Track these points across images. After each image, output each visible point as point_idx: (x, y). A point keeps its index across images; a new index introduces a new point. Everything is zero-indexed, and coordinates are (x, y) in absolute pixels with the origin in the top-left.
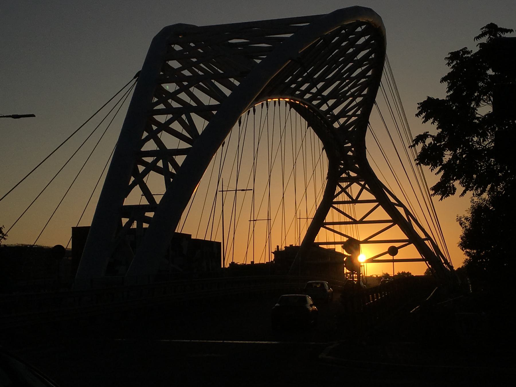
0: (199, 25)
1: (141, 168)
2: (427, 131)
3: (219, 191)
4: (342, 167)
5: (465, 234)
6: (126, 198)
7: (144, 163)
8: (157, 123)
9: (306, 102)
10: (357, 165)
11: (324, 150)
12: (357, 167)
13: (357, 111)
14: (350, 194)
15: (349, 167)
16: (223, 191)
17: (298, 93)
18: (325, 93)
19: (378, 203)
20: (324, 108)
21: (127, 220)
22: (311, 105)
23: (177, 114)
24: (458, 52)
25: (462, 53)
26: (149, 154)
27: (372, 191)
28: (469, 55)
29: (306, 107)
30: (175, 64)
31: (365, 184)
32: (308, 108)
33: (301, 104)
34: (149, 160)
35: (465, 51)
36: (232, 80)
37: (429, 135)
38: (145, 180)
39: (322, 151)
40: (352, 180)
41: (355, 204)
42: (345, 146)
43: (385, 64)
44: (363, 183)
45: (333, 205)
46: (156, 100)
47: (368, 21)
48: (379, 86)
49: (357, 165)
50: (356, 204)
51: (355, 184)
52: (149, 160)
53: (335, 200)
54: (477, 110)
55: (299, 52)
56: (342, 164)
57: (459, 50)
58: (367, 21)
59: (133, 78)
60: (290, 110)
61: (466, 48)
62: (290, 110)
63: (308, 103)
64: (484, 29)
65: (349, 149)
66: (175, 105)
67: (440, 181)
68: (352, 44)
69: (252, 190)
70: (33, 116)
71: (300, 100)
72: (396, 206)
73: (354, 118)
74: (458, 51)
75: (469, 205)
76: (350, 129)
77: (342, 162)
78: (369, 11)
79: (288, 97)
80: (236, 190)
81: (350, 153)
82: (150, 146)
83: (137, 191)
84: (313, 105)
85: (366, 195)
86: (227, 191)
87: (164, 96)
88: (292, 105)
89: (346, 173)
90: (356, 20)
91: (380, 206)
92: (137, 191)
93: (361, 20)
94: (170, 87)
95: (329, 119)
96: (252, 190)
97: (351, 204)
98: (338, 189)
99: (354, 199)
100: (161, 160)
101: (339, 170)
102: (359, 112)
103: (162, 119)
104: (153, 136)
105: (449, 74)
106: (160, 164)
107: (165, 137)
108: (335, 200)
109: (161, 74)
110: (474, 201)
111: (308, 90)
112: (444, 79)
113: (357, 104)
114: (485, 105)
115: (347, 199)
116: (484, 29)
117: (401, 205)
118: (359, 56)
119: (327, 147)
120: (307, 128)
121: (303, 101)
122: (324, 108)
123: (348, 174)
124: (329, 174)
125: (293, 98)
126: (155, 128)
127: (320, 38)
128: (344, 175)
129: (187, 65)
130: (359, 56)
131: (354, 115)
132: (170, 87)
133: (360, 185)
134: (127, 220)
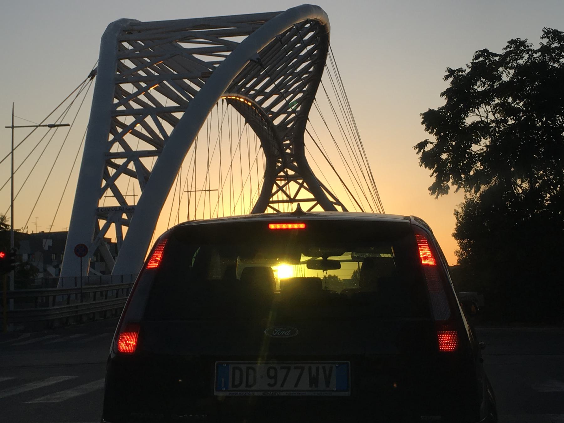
0: (143, 19)
1: (112, 171)
2: (427, 139)
3: (185, 192)
4: (280, 165)
5: (458, 226)
6: (100, 198)
7: (114, 166)
8: (122, 125)
9: (249, 99)
10: (295, 164)
11: (262, 148)
12: (295, 165)
13: (297, 107)
14: (289, 194)
15: (286, 165)
16: (188, 192)
17: (252, 92)
18: (268, 90)
19: (315, 202)
20: (265, 105)
21: (105, 221)
22: (254, 102)
23: (140, 116)
24: (455, 71)
25: (457, 71)
26: (118, 155)
27: (310, 190)
28: (463, 74)
29: (248, 104)
30: (128, 63)
31: (303, 183)
32: (252, 106)
33: (246, 102)
34: (120, 162)
35: (460, 70)
36: (186, 81)
37: (429, 142)
38: (116, 183)
39: (259, 147)
40: (289, 179)
41: (293, 203)
42: (284, 143)
43: (328, 61)
44: (300, 181)
45: (270, 204)
46: (116, 101)
47: (317, 19)
48: (320, 82)
49: (295, 164)
50: (294, 203)
51: (292, 183)
52: (120, 162)
53: (271, 200)
54: (465, 120)
55: (258, 52)
56: (279, 162)
57: (455, 69)
58: (315, 19)
59: (87, 77)
60: (227, 107)
61: (462, 68)
62: (227, 107)
63: (252, 101)
64: (478, 53)
65: (288, 146)
66: (136, 106)
67: (435, 182)
68: (300, 40)
69: (217, 190)
70: (68, 125)
71: (245, 97)
72: (335, 206)
73: (293, 115)
74: (454, 70)
75: (464, 201)
76: (289, 126)
77: (281, 160)
78: (317, 9)
79: (235, 95)
80: (209, 190)
81: (288, 151)
82: (117, 148)
83: (109, 192)
84: (256, 102)
85: (305, 194)
86: (202, 191)
87: (125, 97)
88: (229, 101)
89: (284, 172)
90: (307, 19)
91: (319, 205)
92: (109, 192)
93: (311, 19)
94: (129, 88)
95: (270, 116)
96: (217, 190)
97: (289, 203)
98: (275, 188)
99: (292, 197)
100: (132, 163)
101: (277, 168)
102: (298, 109)
103: (128, 120)
104: (119, 139)
105: (447, 89)
106: (132, 166)
107: (129, 138)
108: (271, 200)
109: (118, 74)
110: (467, 198)
111: (253, 87)
112: (443, 95)
113: (297, 101)
114: (473, 115)
115: (285, 198)
116: (478, 53)
117: (339, 203)
118: (302, 53)
119: (265, 145)
120: (245, 125)
121: (247, 98)
122: (265, 105)
123: (286, 173)
124: (266, 173)
125: (239, 95)
126: (120, 130)
127: (275, 38)
128: (282, 174)
129: (141, 65)
130: (302, 53)
131: (294, 111)
132: (129, 88)
133: (298, 183)
134: (105, 221)
